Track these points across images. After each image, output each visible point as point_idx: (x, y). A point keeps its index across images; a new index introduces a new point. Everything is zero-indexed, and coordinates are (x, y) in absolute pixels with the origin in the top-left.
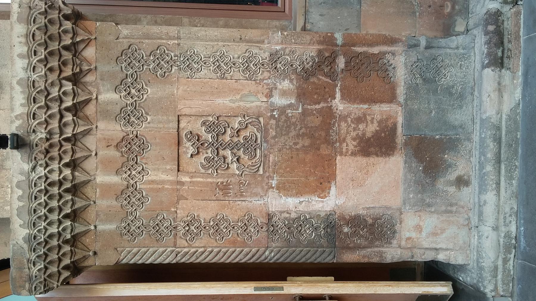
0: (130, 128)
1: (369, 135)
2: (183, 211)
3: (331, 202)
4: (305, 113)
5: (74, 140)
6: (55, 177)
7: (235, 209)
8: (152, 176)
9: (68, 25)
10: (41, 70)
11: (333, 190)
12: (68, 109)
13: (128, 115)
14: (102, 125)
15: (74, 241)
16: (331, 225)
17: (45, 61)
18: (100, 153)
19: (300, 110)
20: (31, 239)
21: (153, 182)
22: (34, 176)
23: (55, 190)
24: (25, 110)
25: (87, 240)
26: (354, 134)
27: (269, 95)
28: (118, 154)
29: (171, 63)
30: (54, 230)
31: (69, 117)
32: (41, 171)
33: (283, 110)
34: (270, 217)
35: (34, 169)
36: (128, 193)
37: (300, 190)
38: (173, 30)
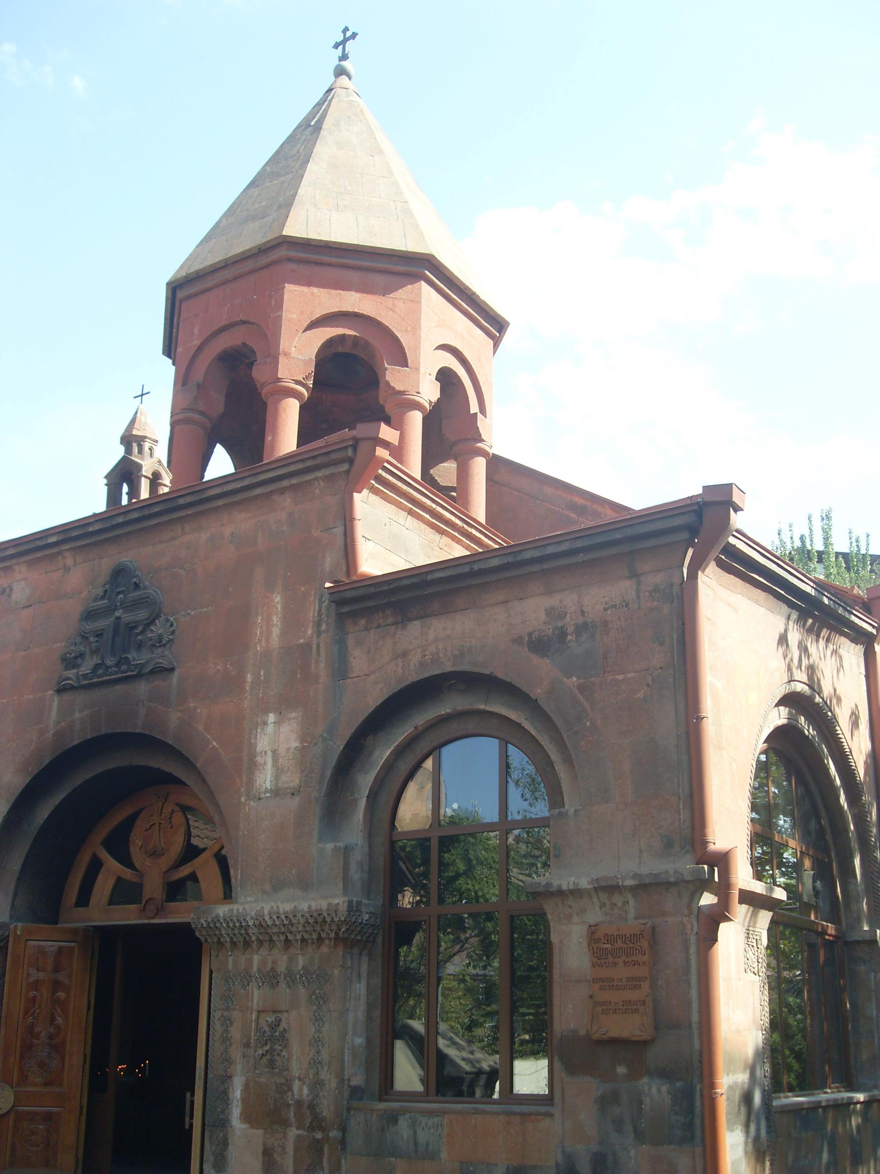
0: (282, 976)
1: (275, 1156)
2: (236, 1014)
3: (237, 1122)
4: (289, 1105)
5: (271, 940)
6: (250, 932)
7: (236, 1053)
8: (256, 993)
9: (333, 935)
10: (302, 921)
11: (244, 1126)
12: (287, 936)
13: (290, 975)
16: (223, 1123)
18: (270, 957)
19: (291, 1102)
21: (253, 993)
23: (243, 932)
26: (276, 1144)
27: (300, 1079)
28: (269, 969)
30: (223, 932)
31: (283, 938)
32: (251, 923)
33: (290, 1088)
34: (230, 1077)
35: (252, 918)
36: (246, 977)
37: (245, 1100)
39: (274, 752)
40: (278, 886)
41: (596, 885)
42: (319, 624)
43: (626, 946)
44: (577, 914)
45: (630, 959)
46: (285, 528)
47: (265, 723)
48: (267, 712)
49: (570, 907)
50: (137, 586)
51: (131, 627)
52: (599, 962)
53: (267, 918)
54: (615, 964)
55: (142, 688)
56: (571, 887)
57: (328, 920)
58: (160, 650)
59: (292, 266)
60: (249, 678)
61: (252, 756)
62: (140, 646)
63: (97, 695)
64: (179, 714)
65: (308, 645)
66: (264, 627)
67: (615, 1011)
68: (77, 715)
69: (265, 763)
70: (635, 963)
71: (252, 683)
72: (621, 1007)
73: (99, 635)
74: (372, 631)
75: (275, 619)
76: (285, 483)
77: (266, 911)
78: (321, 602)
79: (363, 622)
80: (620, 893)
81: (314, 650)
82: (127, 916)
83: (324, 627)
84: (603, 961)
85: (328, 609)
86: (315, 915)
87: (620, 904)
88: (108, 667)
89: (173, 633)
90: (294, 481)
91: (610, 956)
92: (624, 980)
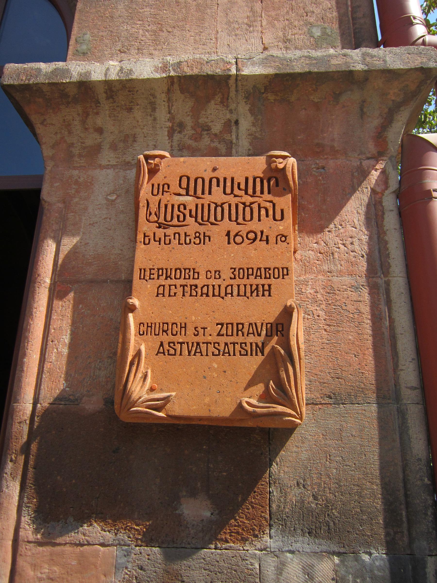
41: (172, 73)
43: (233, 201)
44: (114, 147)
45: (244, 229)
49: (100, 131)
52: (160, 233)
54: (203, 238)
56: (113, 76)
67: (196, 349)
70: (255, 237)
72: (214, 338)
80: (225, 101)
84: (170, 231)
87: (217, 128)
91: (190, 220)
92: (226, 274)
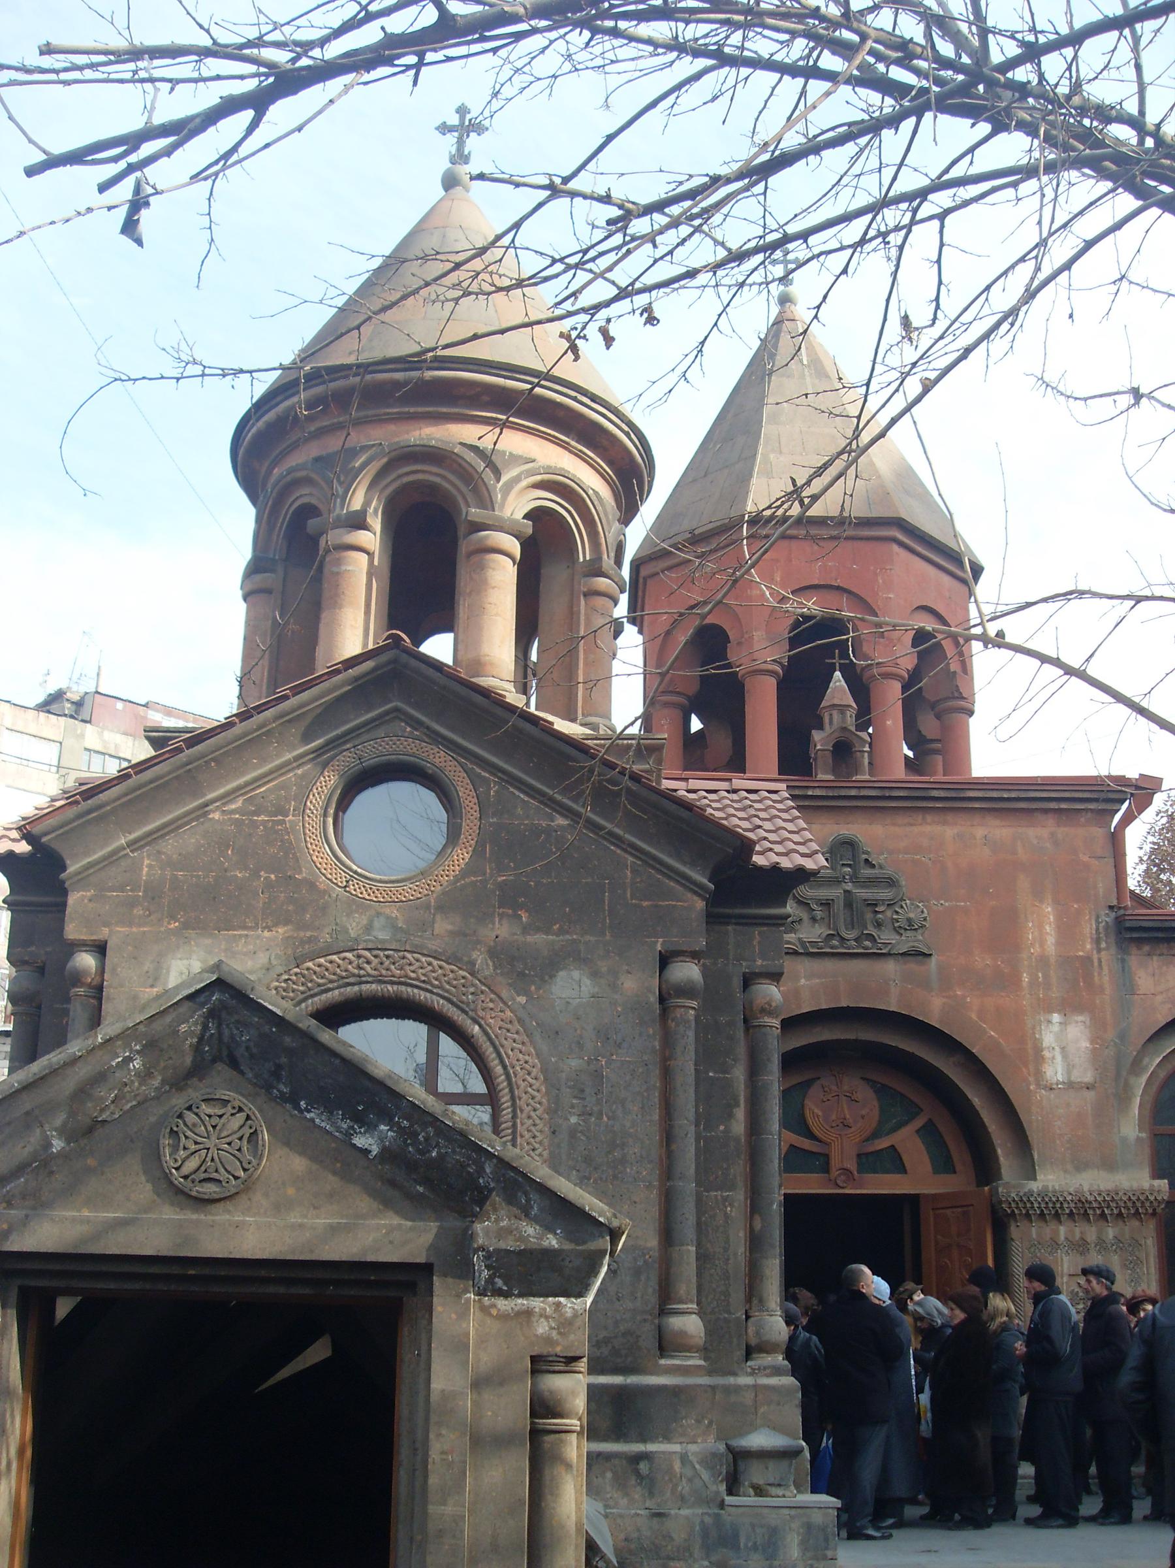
5: (1086, 1214)
6: (1065, 1205)
8: (1065, 1259)
9: (1150, 1211)
14: (1094, 1229)
15: (1028, 1215)
17: (1130, 1199)
20: (1031, 1193)
22: (1065, 1194)
23: (1058, 1205)
24: (1102, 1188)
25: (1026, 1222)
29: (1133, 1270)
30: (1036, 1205)
31: (1098, 1212)
32: (1069, 1198)
38: (1153, 1270)
39: (1063, 1049)
40: (1080, 1166)
42: (1098, 941)
46: (1048, 845)
47: (1049, 1022)
48: (1050, 1010)
50: (867, 860)
51: (873, 905)
53: (1087, 1195)
55: (890, 967)
57: (1152, 1198)
58: (909, 933)
59: (895, 548)
60: (1025, 978)
61: (1038, 1050)
62: (879, 925)
63: (829, 965)
64: (945, 1000)
65: (1088, 959)
66: (1036, 933)
68: (803, 981)
69: (1053, 1058)
71: (1029, 982)
73: (827, 904)
74: (1155, 958)
75: (1047, 928)
76: (1053, 805)
77: (1086, 1188)
78: (1098, 922)
79: (1146, 948)
81: (1096, 963)
82: (811, 1185)
83: (1103, 945)
85: (1107, 927)
86: (1138, 1193)
88: (843, 939)
89: (925, 919)
90: (1064, 806)
